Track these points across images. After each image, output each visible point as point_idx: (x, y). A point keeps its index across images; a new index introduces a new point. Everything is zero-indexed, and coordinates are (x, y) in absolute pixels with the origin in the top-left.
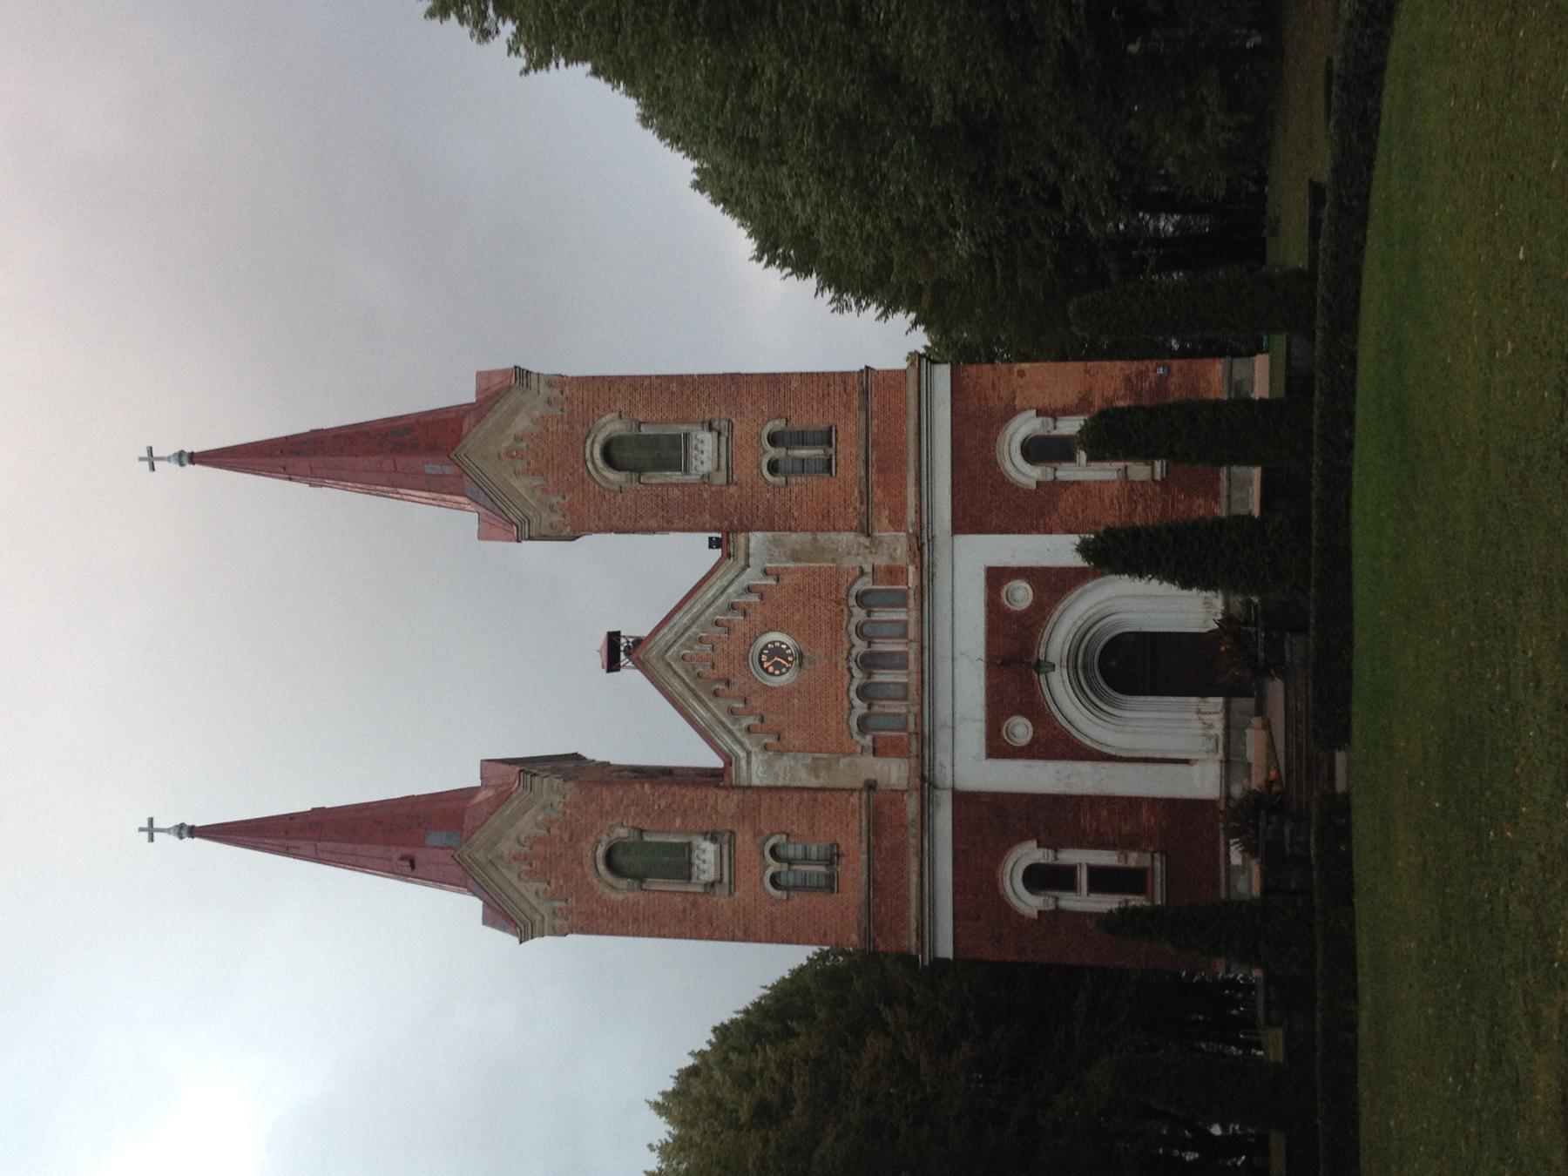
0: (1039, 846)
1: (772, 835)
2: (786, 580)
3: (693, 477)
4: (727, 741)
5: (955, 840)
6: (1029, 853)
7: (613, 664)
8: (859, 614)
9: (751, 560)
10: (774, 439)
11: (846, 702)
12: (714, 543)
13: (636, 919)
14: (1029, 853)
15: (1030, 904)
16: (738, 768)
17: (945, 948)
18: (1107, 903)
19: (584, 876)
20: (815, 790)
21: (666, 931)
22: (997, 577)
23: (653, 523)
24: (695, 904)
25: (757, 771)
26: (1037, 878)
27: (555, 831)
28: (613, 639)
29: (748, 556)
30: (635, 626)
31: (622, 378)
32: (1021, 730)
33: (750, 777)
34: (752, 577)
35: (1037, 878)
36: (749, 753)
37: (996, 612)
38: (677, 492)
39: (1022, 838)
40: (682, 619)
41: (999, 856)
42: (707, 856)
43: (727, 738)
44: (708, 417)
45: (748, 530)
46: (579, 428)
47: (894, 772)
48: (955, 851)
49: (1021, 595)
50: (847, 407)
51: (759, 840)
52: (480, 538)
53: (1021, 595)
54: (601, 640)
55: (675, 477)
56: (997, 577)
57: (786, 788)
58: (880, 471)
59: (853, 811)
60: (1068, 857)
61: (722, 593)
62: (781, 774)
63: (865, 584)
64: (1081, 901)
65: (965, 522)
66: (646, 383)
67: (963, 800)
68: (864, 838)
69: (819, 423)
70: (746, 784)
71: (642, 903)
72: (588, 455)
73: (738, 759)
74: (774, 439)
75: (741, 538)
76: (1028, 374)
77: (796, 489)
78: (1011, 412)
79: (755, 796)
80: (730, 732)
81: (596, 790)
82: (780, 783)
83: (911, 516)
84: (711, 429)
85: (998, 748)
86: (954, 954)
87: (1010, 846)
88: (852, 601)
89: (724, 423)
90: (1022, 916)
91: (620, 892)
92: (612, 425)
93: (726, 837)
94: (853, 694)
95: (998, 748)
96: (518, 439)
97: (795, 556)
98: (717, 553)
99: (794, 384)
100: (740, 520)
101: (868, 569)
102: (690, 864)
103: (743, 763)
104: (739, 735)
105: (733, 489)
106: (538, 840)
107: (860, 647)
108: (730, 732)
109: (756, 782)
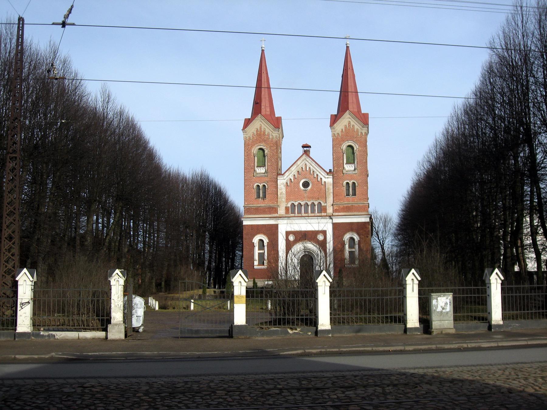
0: (268, 242)
1: (267, 185)
2: (323, 186)
3: (345, 166)
4: (287, 174)
5: (268, 225)
6: (266, 241)
7: (304, 147)
8: (316, 203)
9: (327, 179)
10: (354, 183)
11: (297, 200)
12: (330, 170)
13: (248, 155)
14: (266, 241)
15: (256, 240)
16: (281, 177)
17: (245, 223)
18: (256, 257)
19: (257, 143)
20: (277, 194)
21: (246, 162)
22: (324, 233)
23: (335, 156)
24: (252, 168)
25: (282, 182)
26: (261, 241)
27: (266, 136)
28: (310, 147)
29: (328, 178)
30: (312, 151)
31: (366, 149)
32: (291, 238)
33: (279, 180)
34: (324, 180)
35: (261, 241)
36: (285, 179)
37: (317, 232)
38: (341, 162)
39: (269, 239)
40: (313, 164)
41: (265, 234)
42: (261, 170)
43: (288, 174)
44: (358, 168)
45: (333, 178)
46: (355, 139)
47: (282, 211)
48: (265, 225)
49: (321, 237)
50: (360, 199)
51: (266, 182)
52: (332, 115)
53: (321, 237)
54: (310, 144)
55: (345, 162)
56: (324, 233)
57: (277, 188)
58: (347, 207)
59: (273, 203)
60: (266, 248)
61: (319, 173)
62: (280, 187)
63: (323, 204)
64: (257, 251)
65: (335, 226)
66: (365, 154)
67: (276, 226)
68: (268, 205)
69: (357, 193)
70: (278, 179)
71: (252, 157)
72: (349, 141)
73: (283, 177)
74: (354, 183)
75: (332, 177)
76: (368, 239)
77: (342, 188)
78: (359, 234)
79: (276, 181)
80: (289, 175)
81: (276, 146)
82: (278, 186)
83: (337, 214)
84: (355, 169)
85: (288, 233)
86: (244, 225)
87: (267, 236)
88: (318, 201)
89: (357, 172)
90: (253, 239)
91: (255, 150)
92: (356, 147)
93: (266, 175)
94: (298, 202)
95: (288, 233)
96: (353, 126)
97: (328, 188)
98: (328, 171)
99: (365, 187)
100: (335, 176)
101: (325, 204)
102: (260, 167)
103: (282, 178)
104: (289, 177)
105: (342, 174)
106: (264, 132)
107: (309, 203)
108: (289, 175)
109: (279, 181)
